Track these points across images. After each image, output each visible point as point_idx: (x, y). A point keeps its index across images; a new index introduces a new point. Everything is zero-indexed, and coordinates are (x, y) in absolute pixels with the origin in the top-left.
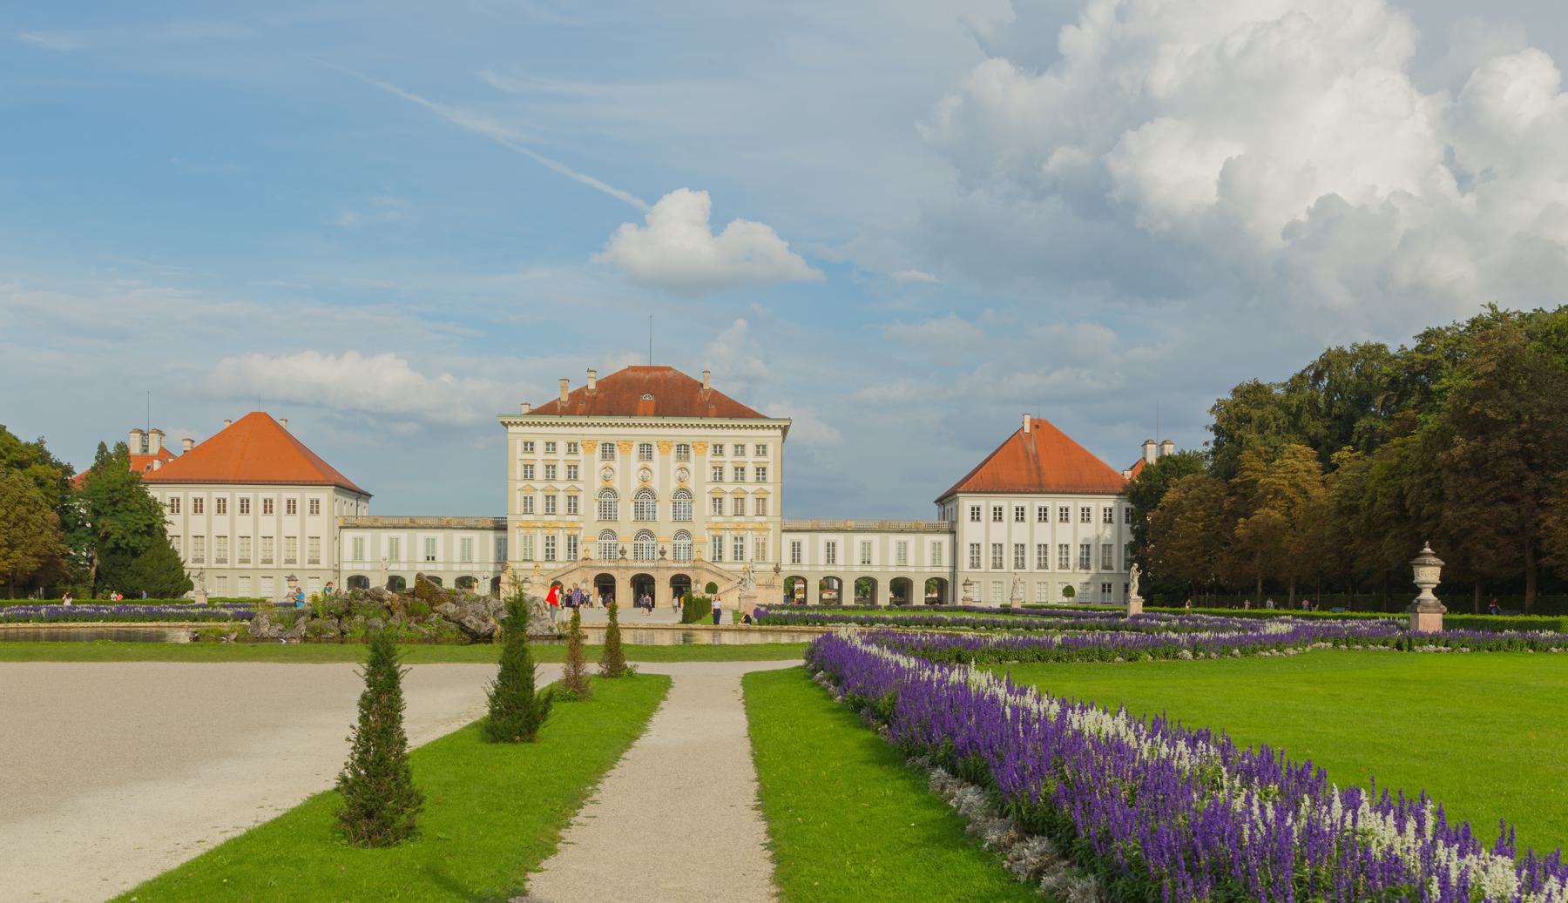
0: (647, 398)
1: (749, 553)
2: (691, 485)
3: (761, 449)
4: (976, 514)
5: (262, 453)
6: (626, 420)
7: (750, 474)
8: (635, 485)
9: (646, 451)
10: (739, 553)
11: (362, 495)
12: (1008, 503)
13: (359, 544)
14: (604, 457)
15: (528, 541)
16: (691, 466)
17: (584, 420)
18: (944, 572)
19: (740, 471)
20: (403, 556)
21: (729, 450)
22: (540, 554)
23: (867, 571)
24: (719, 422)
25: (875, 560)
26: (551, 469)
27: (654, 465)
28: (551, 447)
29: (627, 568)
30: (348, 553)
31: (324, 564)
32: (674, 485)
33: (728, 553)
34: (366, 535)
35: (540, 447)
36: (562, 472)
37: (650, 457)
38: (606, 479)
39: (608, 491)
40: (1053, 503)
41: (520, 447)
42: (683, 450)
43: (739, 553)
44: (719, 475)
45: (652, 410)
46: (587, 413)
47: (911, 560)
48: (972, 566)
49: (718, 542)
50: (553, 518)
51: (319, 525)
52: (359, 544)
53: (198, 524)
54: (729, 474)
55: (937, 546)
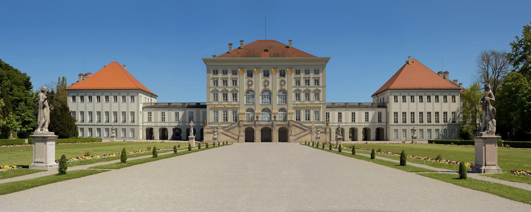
1: (312, 118)
4: (396, 101)
7: (312, 82)
8: (261, 88)
10: (308, 118)
11: (155, 96)
16: (286, 80)
19: (307, 82)
22: (221, 119)
23: (354, 125)
26: (225, 82)
27: (270, 79)
29: (260, 125)
30: (146, 120)
31: (136, 123)
32: (278, 88)
38: (248, 85)
42: (283, 74)
44: (298, 82)
48: (395, 122)
49: (298, 113)
50: (226, 103)
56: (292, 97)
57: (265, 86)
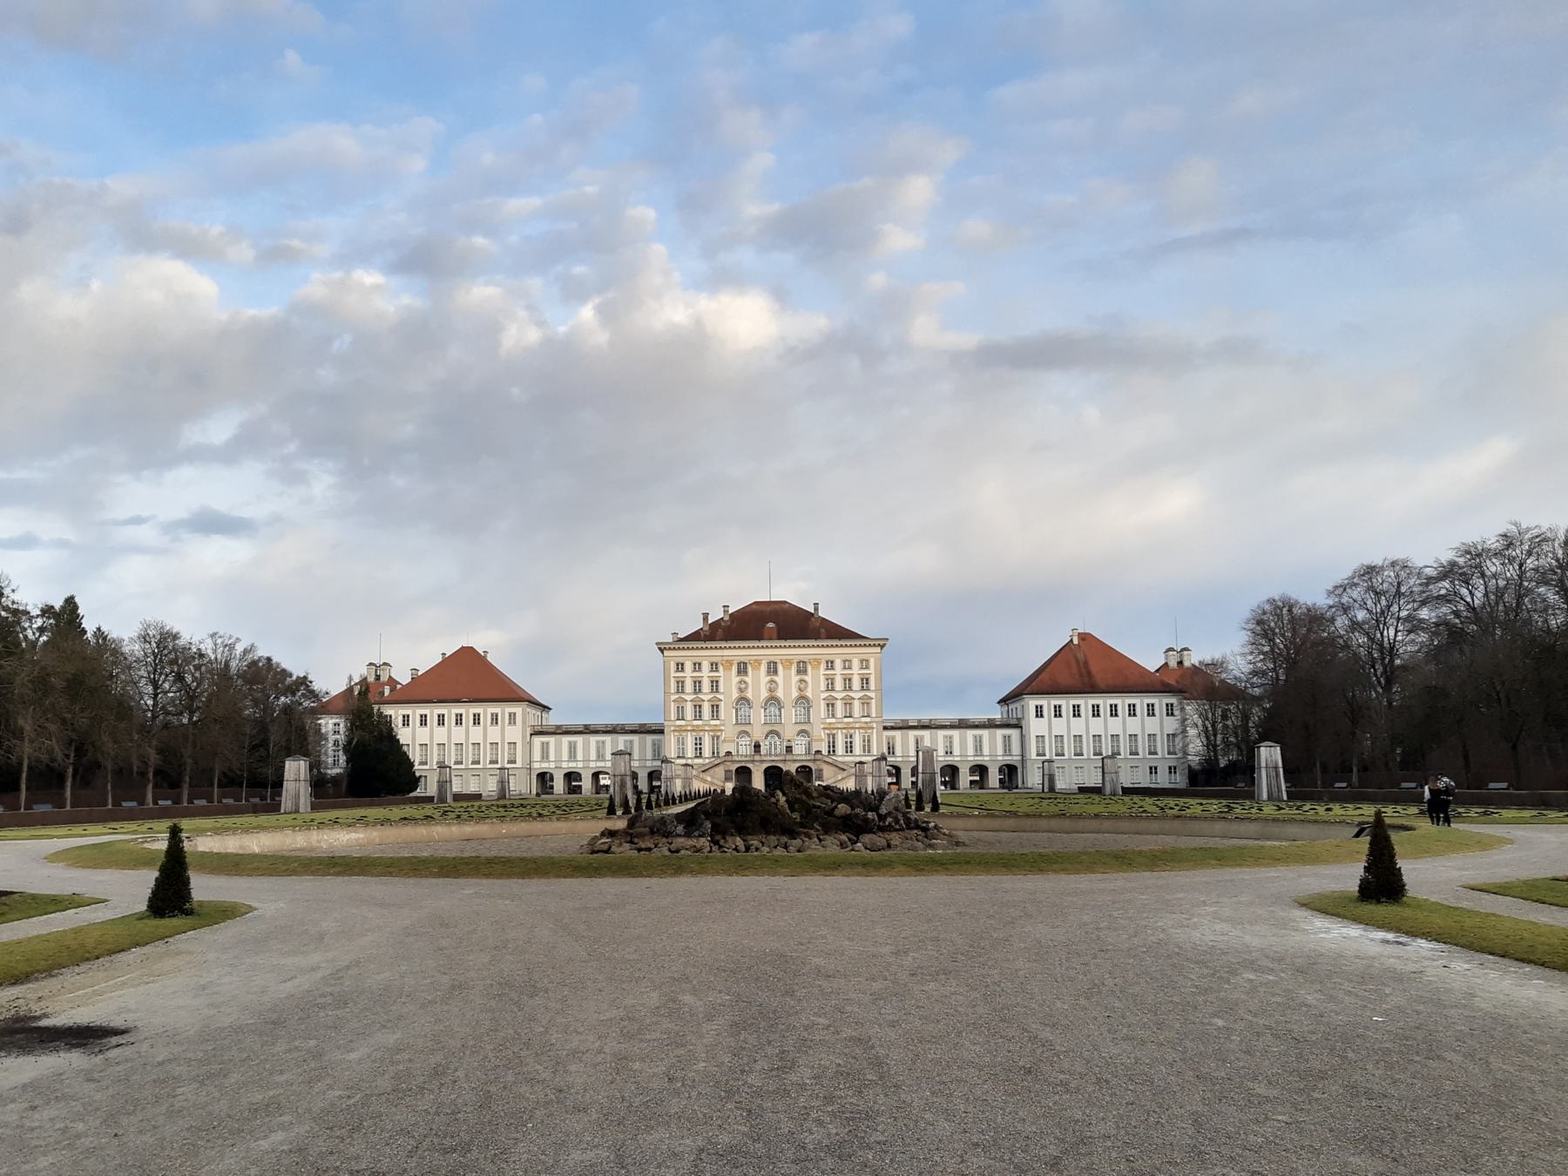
0: (771, 625)
1: (858, 749)
2: (809, 694)
3: (865, 664)
4: (1039, 712)
5: (467, 679)
6: (756, 643)
7: (856, 684)
8: (764, 694)
9: (772, 669)
10: (849, 748)
12: (1066, 703)
13: (545, 747)
14: (739, 672)
15: (681, 742)
17: (723, 644)
18: (1014, 759)
19: (848, 681)
20: (580, 756)
21: (838, 664)
22: (690, 753)
24: (830, 642)
25: (956, 751)
26: (697, 684)
27: (779, 679)
28: (697, 666)
30: (537, 756)
31: (519, 764)
32: (795, 694)
33: (840, 749)
34: (551, 739)
35: (688, 666)
36: (706, 687)
37: (775, 672)
38: (741, 690)
39: (743, 700)
40: (1104, 702)
41: (673, 666)
42: (802, 671)
43: (849, 748)
44: (831, 686)
45: (775, 634)
46: (726, 639)
47: (986, 751)
51: (515, 733)
52: (545, 747)
53: (423, 735)
54: (839, 685)
55: (1007, 739)
56: (820, 710)
57: (770, 690)
